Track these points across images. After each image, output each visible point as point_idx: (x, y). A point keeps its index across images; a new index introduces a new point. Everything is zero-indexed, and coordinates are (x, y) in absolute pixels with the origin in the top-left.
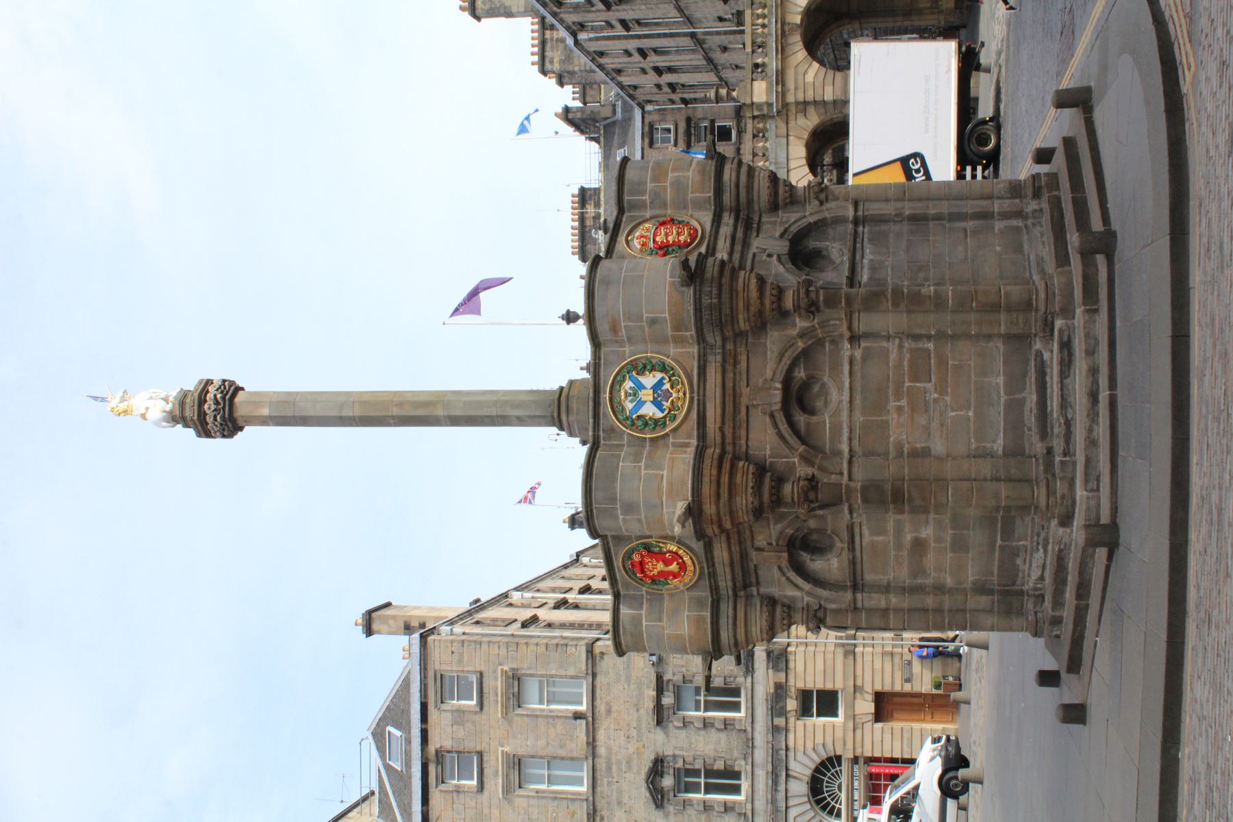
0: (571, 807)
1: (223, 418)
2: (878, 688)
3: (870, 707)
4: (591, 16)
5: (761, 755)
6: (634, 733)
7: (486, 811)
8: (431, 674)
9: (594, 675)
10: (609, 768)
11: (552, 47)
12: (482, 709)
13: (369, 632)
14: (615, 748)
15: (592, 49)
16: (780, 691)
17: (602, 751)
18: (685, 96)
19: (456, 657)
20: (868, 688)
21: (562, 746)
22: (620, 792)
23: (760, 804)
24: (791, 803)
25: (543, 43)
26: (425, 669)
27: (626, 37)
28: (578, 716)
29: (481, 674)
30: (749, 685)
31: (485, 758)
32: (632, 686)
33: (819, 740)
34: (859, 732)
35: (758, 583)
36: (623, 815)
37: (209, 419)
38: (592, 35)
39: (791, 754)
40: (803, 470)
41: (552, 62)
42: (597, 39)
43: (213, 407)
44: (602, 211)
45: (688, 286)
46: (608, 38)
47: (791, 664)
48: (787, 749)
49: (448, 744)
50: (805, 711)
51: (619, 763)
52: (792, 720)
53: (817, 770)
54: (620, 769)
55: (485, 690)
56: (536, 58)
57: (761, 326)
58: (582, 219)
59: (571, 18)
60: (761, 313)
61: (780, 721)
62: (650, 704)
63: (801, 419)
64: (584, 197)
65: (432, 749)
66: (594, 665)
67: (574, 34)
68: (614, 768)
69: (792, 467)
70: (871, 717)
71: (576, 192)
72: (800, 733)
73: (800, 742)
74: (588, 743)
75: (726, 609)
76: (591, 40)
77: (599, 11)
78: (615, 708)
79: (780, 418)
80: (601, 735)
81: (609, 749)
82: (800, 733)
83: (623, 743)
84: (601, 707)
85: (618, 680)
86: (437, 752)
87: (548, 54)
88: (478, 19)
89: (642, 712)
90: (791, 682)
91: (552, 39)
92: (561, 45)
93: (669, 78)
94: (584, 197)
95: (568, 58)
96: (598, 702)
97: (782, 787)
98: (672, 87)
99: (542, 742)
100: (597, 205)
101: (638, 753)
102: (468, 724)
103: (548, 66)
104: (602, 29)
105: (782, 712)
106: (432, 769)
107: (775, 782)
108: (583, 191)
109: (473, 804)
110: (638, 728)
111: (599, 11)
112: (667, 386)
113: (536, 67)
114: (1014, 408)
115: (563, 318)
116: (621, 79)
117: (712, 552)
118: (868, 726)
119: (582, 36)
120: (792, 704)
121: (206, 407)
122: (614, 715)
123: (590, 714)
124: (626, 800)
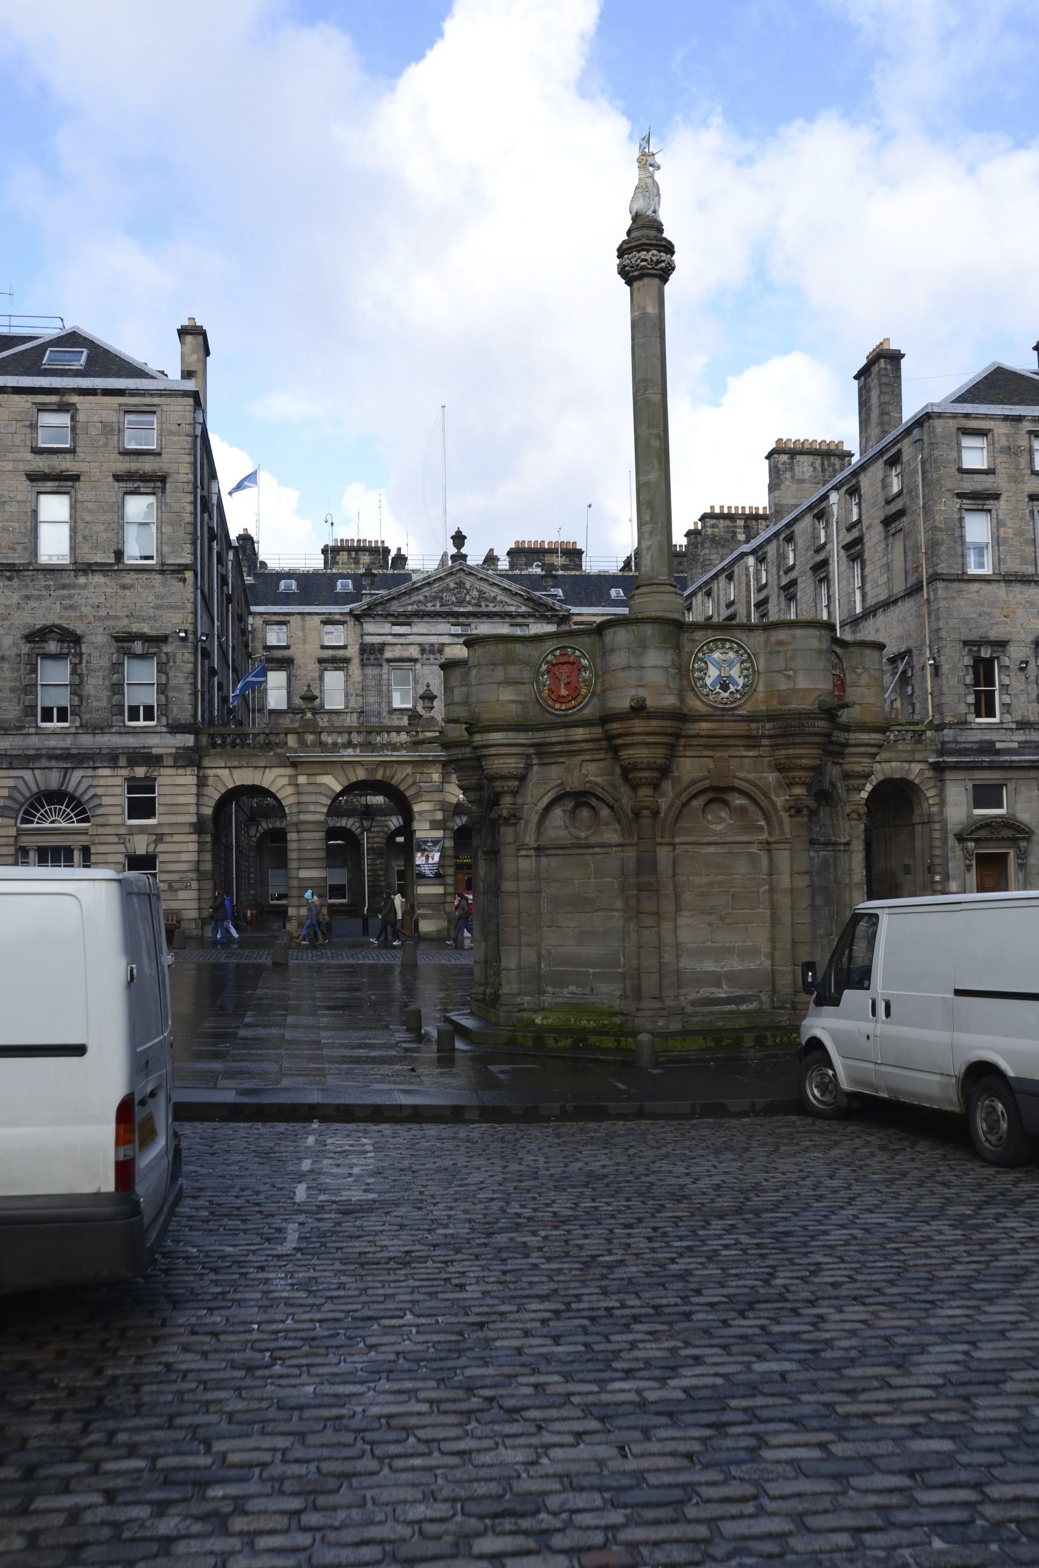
0: (19, 547)
2: (161, 858)
3: (141, 850)
4: (774, 570)
5: (87, 741)
6: (103, 613)
7: (11, 456)
8: (156, 400)
9: (162, 572)
10: (64, 587)
12: (121, 453)
13: (183, 332)
14: (85, 593)
15: (736, 568)
16: (154, 761)
17: (82, 580)
19: (175, 428)
20: (161, 847)
21: (85, 538)
22: (40, 598)
23: (34, 741)
24: (37, 772)
26: (161, 395)
27: (749, 602)
28: (119, 554)
29: (159, 454)
30: (159, 729)
31: (68, 456)
32: (151, 611)
33: (105, 801)
34: (115, 839)
35: (541, 764)
36: (14, 601)
37: (643, 254)
38: (751, 569)
39: (90, 772)
40: (664, 803)
41: (713, 526)
42: (748, 575)
44: (561, 572)
45: (820, 708)
46: (748, 585)
47: (181, 771)
48: (95, 768)
49: (81, 417)
50: (134, 786)
51: (70, 597)
52: (125, 772)
53: (72, 798)
54: (64, 598)
55: (141, 458)
56: (717, 511)
57: (780, 768)
58: (552, 551)
59: (771, 551)
60: (791, 769)
61: (123, 761)
62: (135, 628)
63: (697, 803)
64: (574, 554)
65: (75, 399)
66: (173, 572)
67: (753, 552)
68: (65, 592)
69: (663, 795)
70: (131, 850)
72: (111, 781)
73: (102, 782)
74: (89, 565)
75: (522, 738)
76: (747, 568)
77: (779, 578)
78: (127, 592)
79: (707, 783)
80: (98, 579)
81: (85, 587)
82: (111, 781)
83: (91, 601)
84: (128, 579)
85: (157, 597)
86: (74, 404)
87: (722, 523)
88: (768, 457)
89: (126, 621)
90: (163, 771)
92: (729, 536)
96: (133, 575)
97: (53, 763)
99: (88, 518)
101: (81, 617)
102: (103, 440)
103: (710, 522)
104: (758, 579)
106: (54, 399)
107: (57, 758)
108: (579, 553)
109: (17, 442)
110: (108, 617)
111: (779, 578)
113: (708, 511)
114: (716, 980)
115: (459, 532)
116: (700, 596)
117: (582, 726)
118: (121, 848)
119: (751, 561)
120: (140, 772)
122: (121, 592)
123: (121, 567)
124: (31, 604)
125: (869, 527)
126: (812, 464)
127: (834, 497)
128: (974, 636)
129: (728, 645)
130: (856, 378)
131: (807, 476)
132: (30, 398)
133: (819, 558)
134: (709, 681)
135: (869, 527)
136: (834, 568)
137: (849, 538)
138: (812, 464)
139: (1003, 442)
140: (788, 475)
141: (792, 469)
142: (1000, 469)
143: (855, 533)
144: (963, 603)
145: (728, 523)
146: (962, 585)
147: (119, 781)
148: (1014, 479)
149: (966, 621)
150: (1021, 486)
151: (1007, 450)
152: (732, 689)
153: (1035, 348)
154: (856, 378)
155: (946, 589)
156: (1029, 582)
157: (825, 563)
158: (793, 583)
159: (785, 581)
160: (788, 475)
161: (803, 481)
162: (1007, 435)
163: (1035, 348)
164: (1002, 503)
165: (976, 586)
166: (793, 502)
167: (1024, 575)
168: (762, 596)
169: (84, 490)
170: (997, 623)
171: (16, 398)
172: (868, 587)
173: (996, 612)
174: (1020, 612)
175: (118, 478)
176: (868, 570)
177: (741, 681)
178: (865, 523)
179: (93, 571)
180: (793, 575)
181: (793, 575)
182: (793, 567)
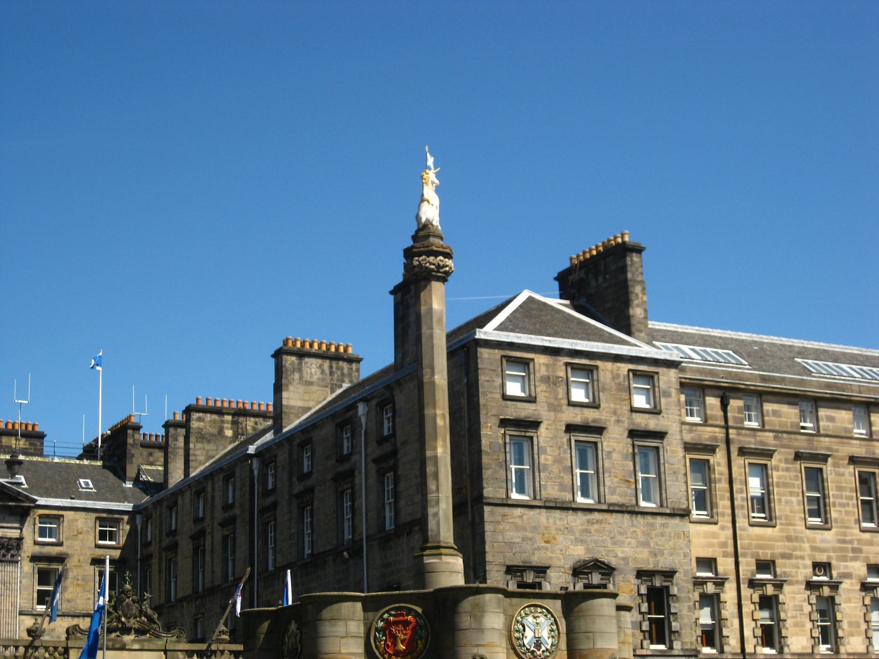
1: (433, 270)
11: (215, 421)
18: (155, 561)
25: (219, 412)
37: (431, 259)
38: (256, 472)
41: (199, 419)
43: (441, 263)
56: (202, 402)
59: (282, 457)
71: (37, 429)
76: (252, 471)
77: (291, 484)
87: (209, 417)
91: (223, 422)
92: (215, 431)
93: (186, 546)
94: (35, 437)
95: (203, 437)
98: (174, 547)
100: (25, 453)
103: (195, 416)
108: (41, 436)
112: (543, 648)
121: (441, 258)
125: (404, 443)
126: (321, 366)
127: (361, 409)
128: (517, 561)
129: (539, 610)
130: (391, 293)
131: (315, 378)
133: (346, 466)
134: (526, 641)
135: (404, 443)
136: (361, 479)
137: (378, 452)
138: (321, 366)
139: (542, 371)
140: (296, 376)
141: (300, 370)
142: (541, 398)
143: (387, 447)
144: (507, 527)
145: (215, 417)
146: (506, 510)
148: (554, 408)
149: (510, 545)
150: (559, 415)
151: (546, 380)
152: (543, 648)
153: (556, 279)
154: (391, 293)
155: (492, 513)
156: (568, 509)
157: (350, 475)
158: (310, 490)
159: (298, 488)
160: (296, 376)
161: (310, 383)
162: (547, 365)
163: (556, 279)
164: (542, 428)
165: (519, 511)
166: (300, 404)
167: (563, 502)
168: (269, 501)
170: (538, 549)
172: (402, 504)
173: (538, 537)
174: (560, 538)
176: (402, 486)
177: (550, 641)
178: (400, 438)
180: (309, 483)
181: (309, 483)
182: (310, 474)
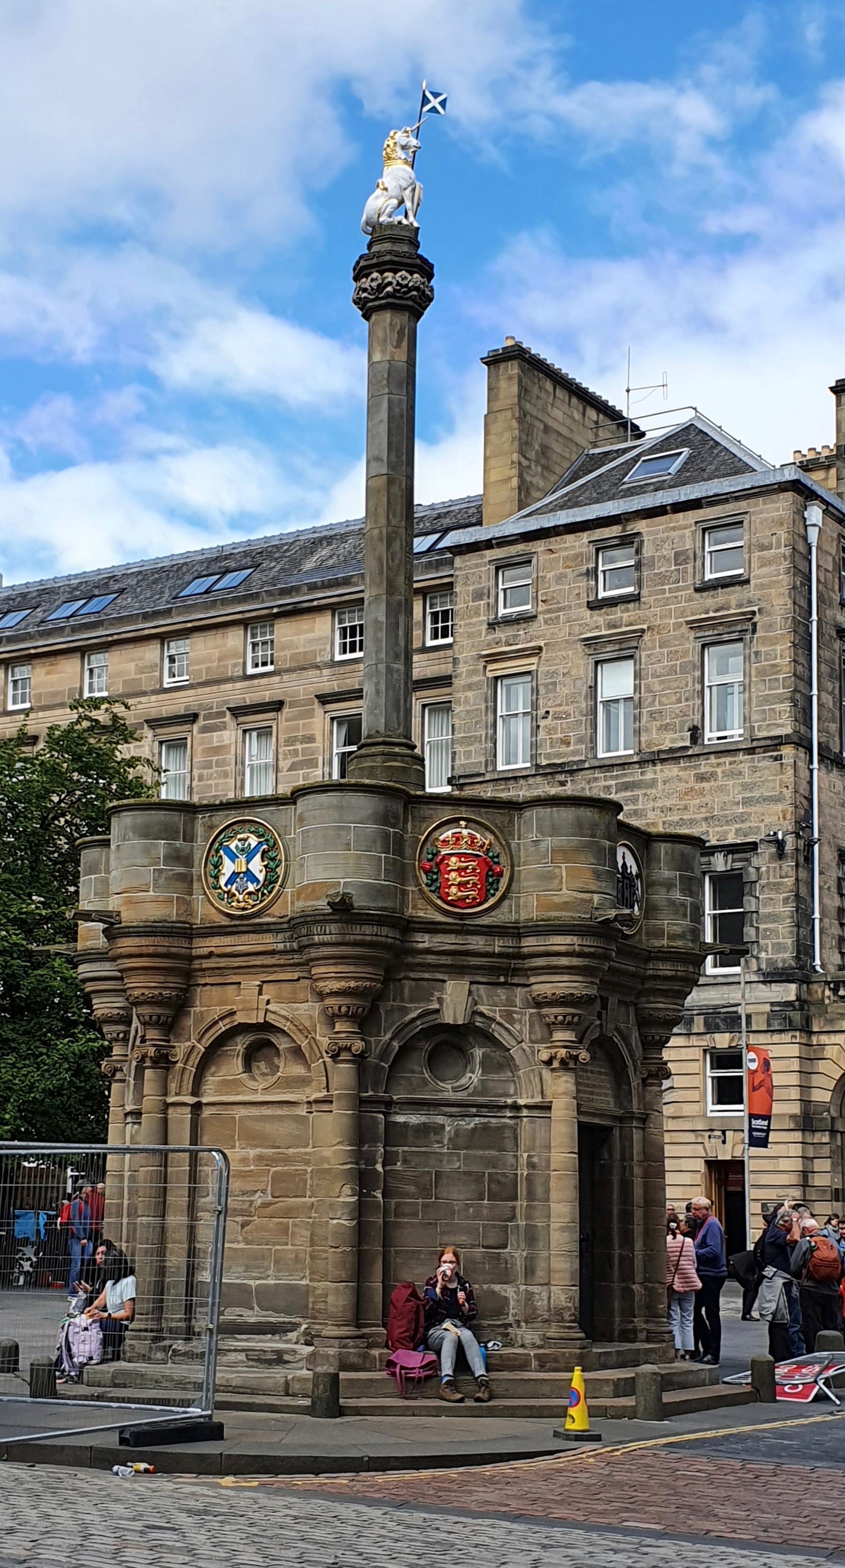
8: (743, 505)
9: (751, 751)
12: (697, 590)
28: (696, 733)
52: (706, 1041)
61: (699, 1024)
65: (641, 526)
66: (766, 748)
74: (660, 752)
80: (671, 770)
81: (653, 783)
83: (659, 804)
84: (705, 766)
96: (713, 759)
105: (711, 1028)
106: (614, 531)
120: (722, 1040)
123: (696, 750)
132: (585, 537)
147: (697, 1054)
169: (651, 650)
171: (570, 538)
175: (696, 625)
179: (663, 761)
